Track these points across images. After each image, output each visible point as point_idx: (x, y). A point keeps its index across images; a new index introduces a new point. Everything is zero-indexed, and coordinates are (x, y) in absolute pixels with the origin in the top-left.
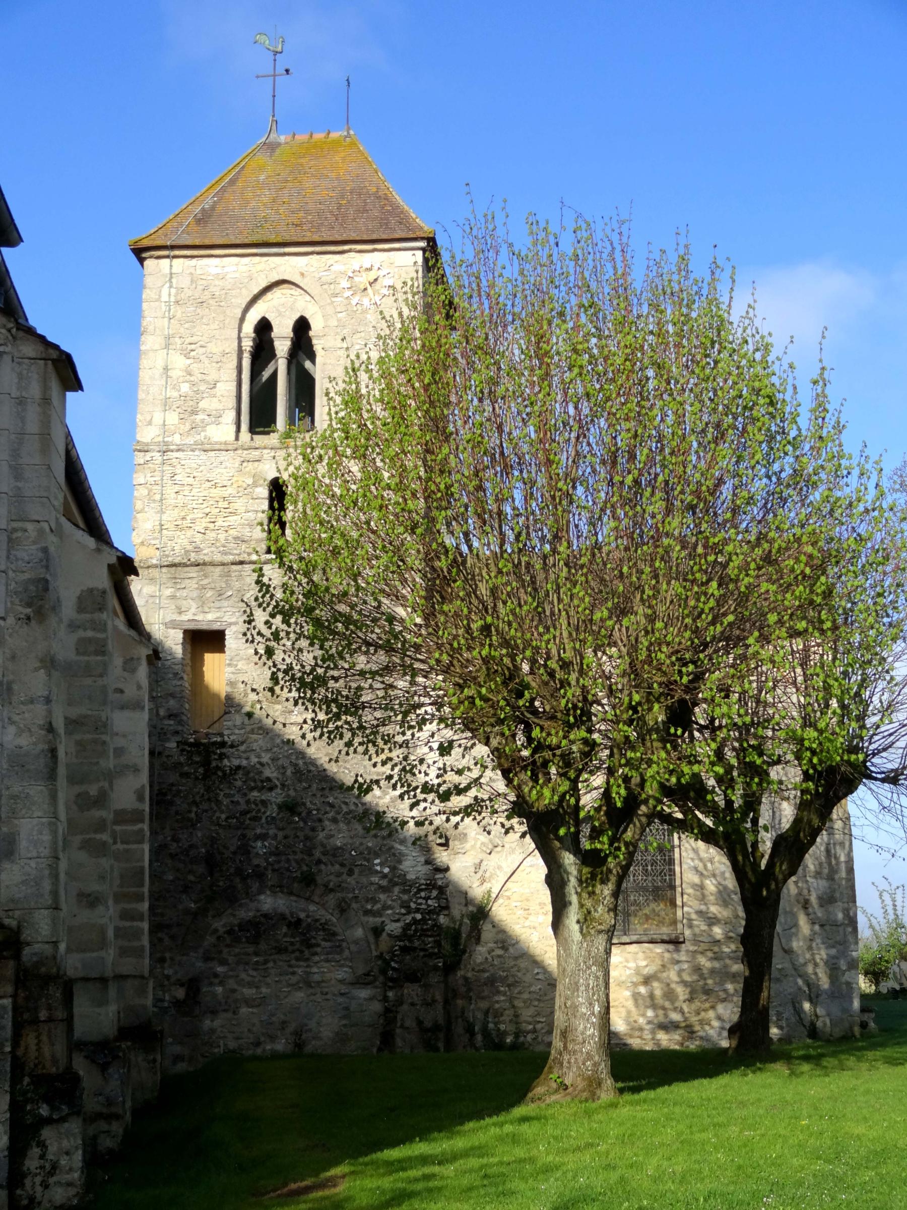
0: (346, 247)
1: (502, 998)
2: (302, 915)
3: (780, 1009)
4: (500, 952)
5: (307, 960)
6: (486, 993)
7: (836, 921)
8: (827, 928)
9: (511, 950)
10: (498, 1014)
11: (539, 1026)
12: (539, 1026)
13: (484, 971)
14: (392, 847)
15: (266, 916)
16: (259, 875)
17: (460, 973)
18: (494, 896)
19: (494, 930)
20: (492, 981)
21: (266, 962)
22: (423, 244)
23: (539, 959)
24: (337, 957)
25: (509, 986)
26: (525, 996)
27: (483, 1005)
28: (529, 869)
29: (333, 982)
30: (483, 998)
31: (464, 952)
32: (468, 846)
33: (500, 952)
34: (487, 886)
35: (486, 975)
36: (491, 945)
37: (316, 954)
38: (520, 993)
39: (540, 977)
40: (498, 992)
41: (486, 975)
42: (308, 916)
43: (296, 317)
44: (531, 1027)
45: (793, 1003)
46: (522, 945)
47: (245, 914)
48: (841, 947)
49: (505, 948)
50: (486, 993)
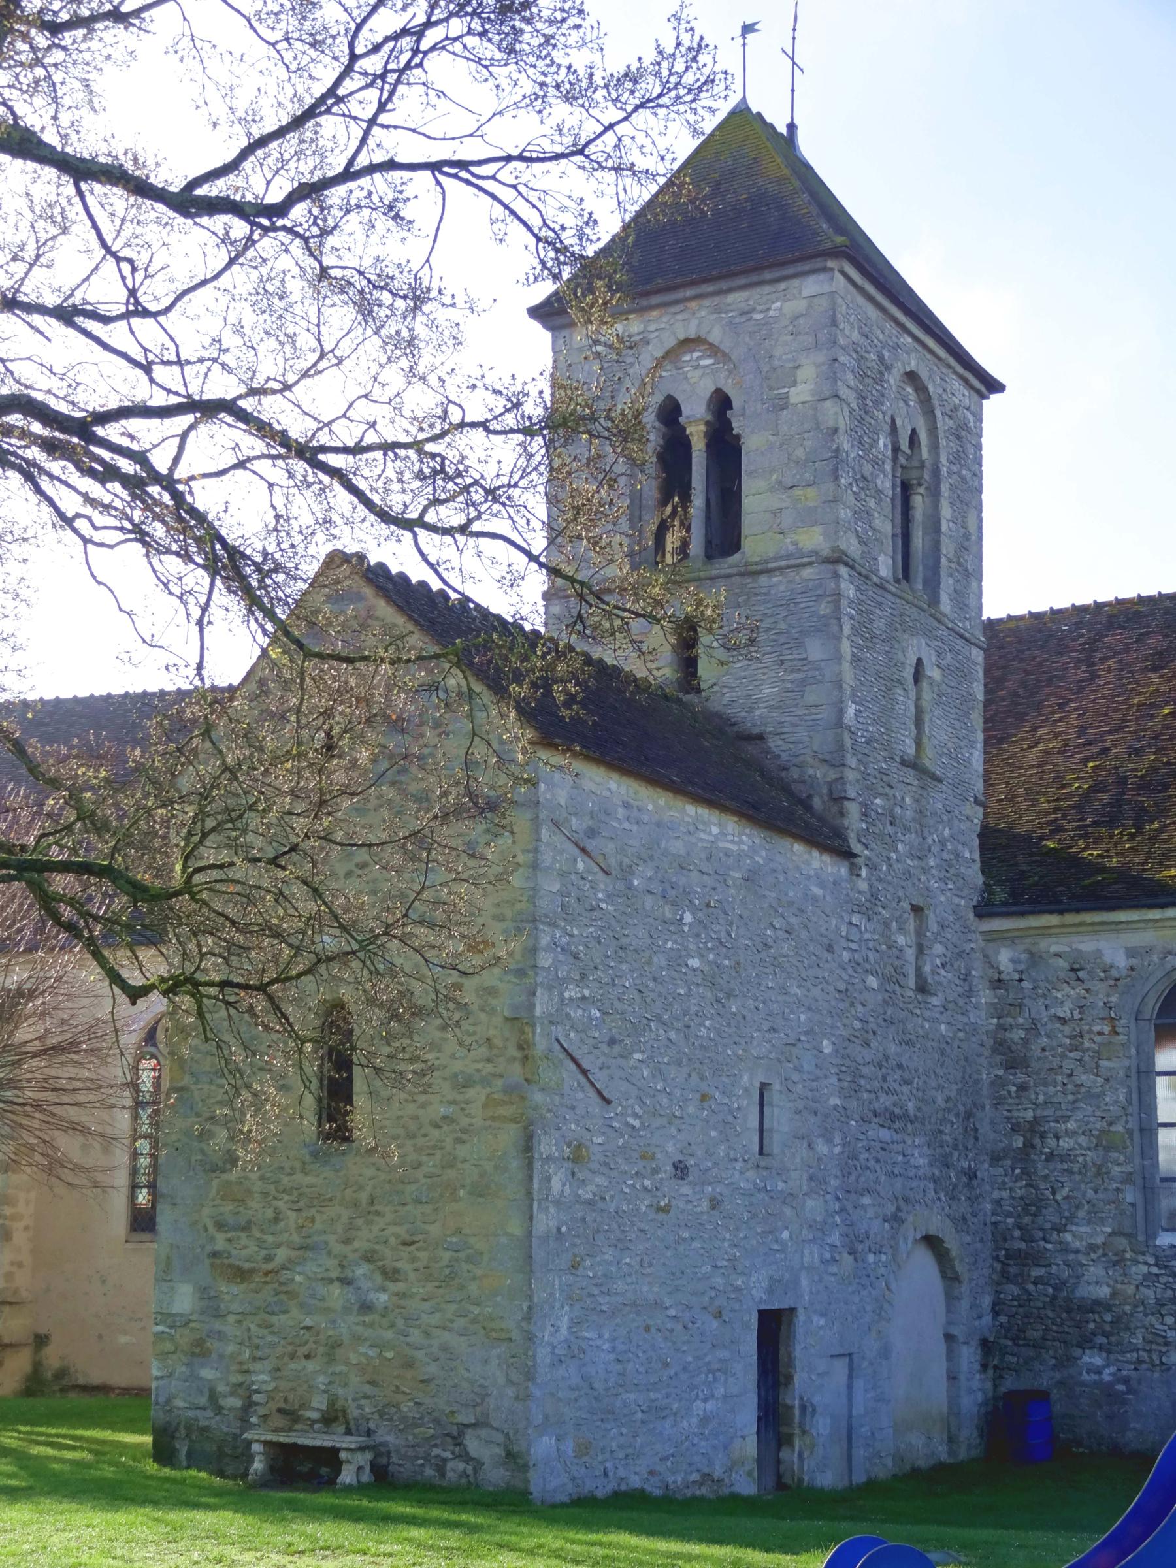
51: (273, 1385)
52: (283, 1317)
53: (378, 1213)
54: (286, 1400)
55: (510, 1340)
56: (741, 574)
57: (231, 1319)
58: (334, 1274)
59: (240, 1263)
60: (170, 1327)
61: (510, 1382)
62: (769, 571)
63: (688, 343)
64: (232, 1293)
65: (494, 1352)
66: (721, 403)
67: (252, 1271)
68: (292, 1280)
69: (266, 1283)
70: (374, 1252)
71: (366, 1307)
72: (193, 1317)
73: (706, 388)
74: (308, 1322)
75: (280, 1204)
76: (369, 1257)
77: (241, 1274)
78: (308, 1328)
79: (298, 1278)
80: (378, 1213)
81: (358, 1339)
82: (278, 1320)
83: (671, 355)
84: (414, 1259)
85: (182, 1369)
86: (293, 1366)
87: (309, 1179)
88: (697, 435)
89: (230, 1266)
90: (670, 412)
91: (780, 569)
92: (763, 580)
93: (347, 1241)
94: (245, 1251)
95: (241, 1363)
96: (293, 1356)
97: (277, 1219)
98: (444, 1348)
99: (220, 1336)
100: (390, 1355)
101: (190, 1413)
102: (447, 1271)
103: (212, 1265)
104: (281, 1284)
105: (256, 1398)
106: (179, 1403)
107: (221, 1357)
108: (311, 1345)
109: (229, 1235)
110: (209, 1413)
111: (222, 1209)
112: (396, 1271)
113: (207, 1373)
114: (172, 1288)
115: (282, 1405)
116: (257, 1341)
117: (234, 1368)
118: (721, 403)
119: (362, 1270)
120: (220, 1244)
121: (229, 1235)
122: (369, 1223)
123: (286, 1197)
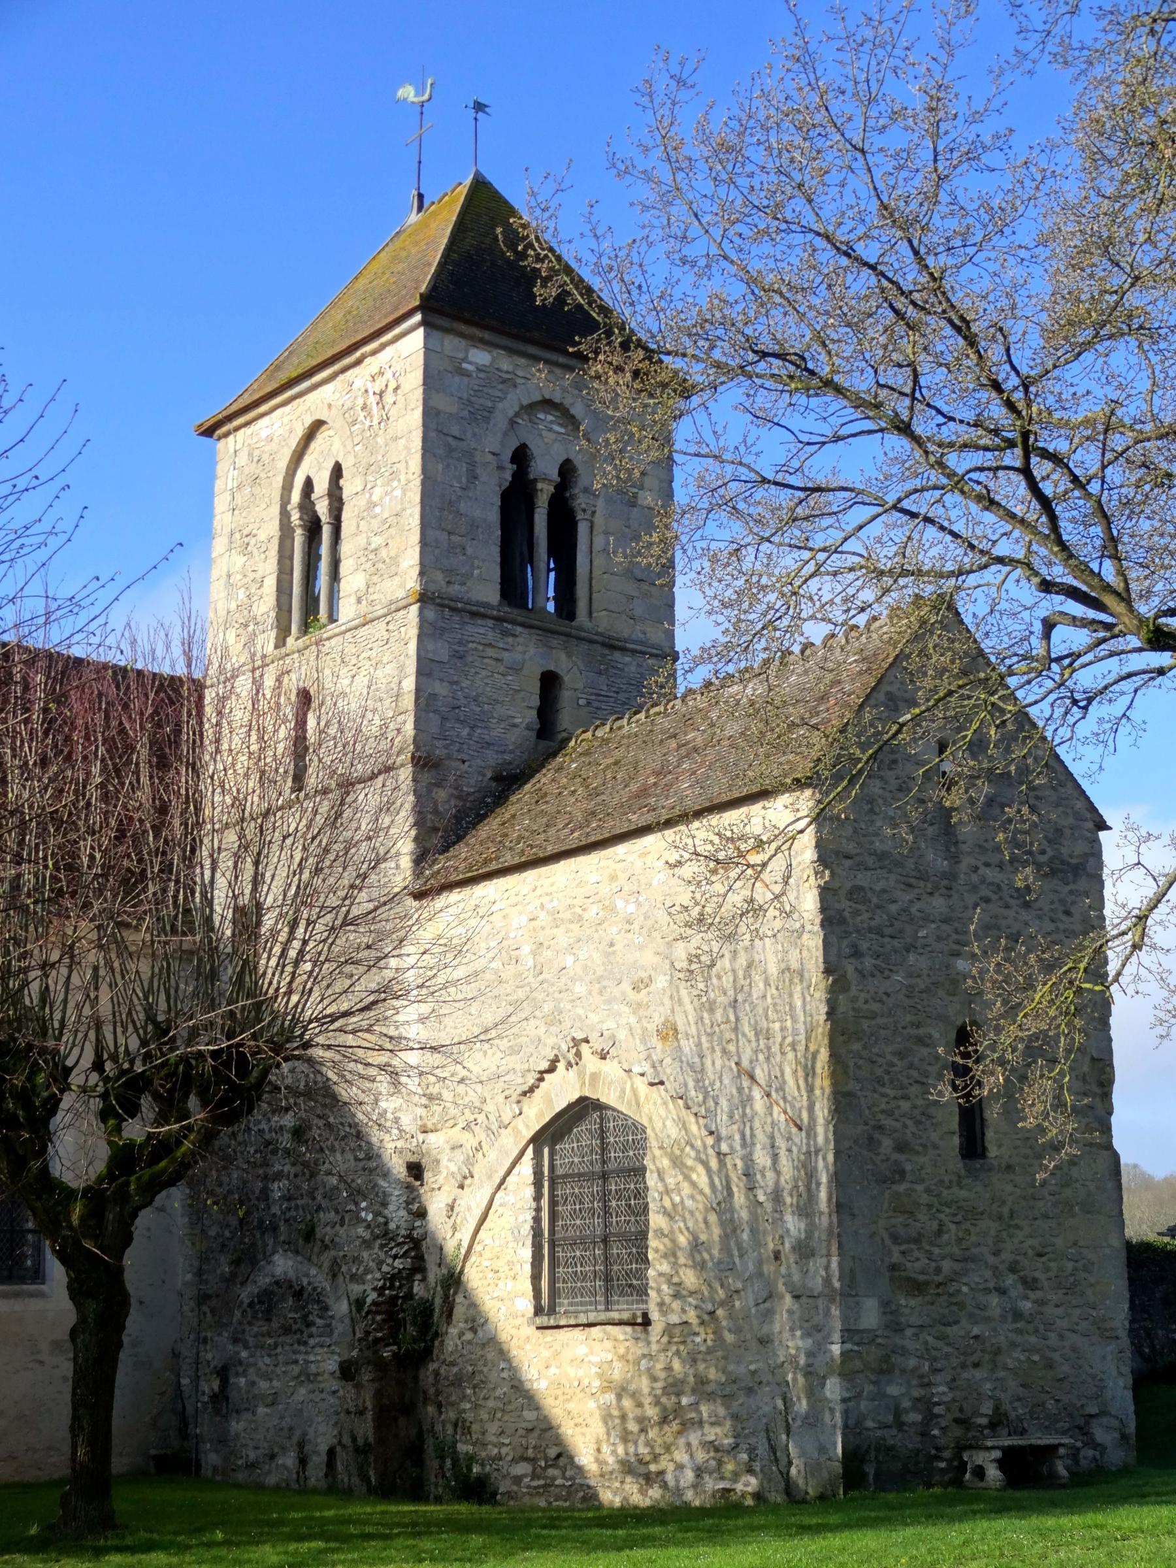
0: (358, 354)
1: (468, 1406)
2: (305, 1281)
3: (752, 1441)
4: (469, 1336)
5: (305, 1343)
6: (453, 1398)
7: (812, 1290)
8: (804, 1300)
9: (480, 1334)
10: (466, 1429)
11: (504, 1450)
12: (504, 1450)
13: (453, 1364)
14: (376, 1185)
15: (277, 1283)
16: (274, 1228)
17: (432, 1366)
18: (463, 1251)
19: (466, 1302)
20: (458, 1382)
21: (276, 1346)
22: (418, 317)
23: (505, 1347)
24: (328, 1341)
25: (474, 1387)
26: (491, 1404)
27: (452, 1415)
28: (501, 1210)
29: (326, 1376)
30: (452, 1404)
31: (436, 1335)
32: (441, 1178)
33: (469, 1336)
34: (458, 1235)
35: (455, 1370)
36: (462, 1325)
37: (311, 1336)
38: (485, 1399)
39: (505, 1375)
40: (464, 1397)
41: (455, 1370)
42: (309, 1283)
43: (332, 464)
44: (496, 1451)
45: (767, 1430)
46: (491, 1326)
47: (264, 1281)
48: (819, 1336)
49: (473, 1330)
50: (453, 1398)
51: (951, 1395)
52: (955, 1328)
53: (1017, 1227)
54: (961, 1410)
55: (1117, 1338)
56: (604, 645)
57: (909, 1332)
58: (991, 1285)
59: (913, 1275)
60: (858, 1344)
61: (1120, 1374)
62: (623, 650)
63: (547, 404)
64: (910, 1307)
65: (1109, 1349)
66: (567, 470)
67: (927, 1284)
68: (959, 1291)
69: (938, 1294)
70: (1016, 1262)
71: (1018, 1315)
72: (879, 1333)
73: (559, 453)
74: (976, 1331)
75: (942, 1216)
76: (1013, 1269)
77: (917, 1287)
78: (976, 1337)
79: (965, 1289)
80: (1017, 1227)
81: (1013, 1345)
82: (952, 1331)
83: (531, 408)
84: (1048, 1270)
85: (869, 1388)
86: (965, 1375)
87: (964, 1194)
88: (545, 492)
89: (908, 1279)
90: (521, 456)
91: (634, 651)
92: (617, 655)
93: (997, 1253)
94: (916, 1266)
95: (921, 1377)
96: (963, 1366)
97: (940, 1232)
98: (1074, 1349)
99: (904, 1352)
100: (1036, 1358)
101: (879, 1433)
102: (1072, 1279)
103: (892, 1279)
104: (951, 1295)
105: (937, 1410)
106: (870, 1424)
107: (903, 1371)
108: (979, 1354)
109: (904, 1247)
110: (894, 1431)
111: (893, 1221)
112: (1035, 1280)
113: (893, 1390)
114: (857, 1303)
115: (957, 1415)
116: (934, 1353)
117: (914, 1382)
118: (567, 470)
119: (1010, 1280)
120: (896, 1257)
121: (904, 1247)
122: (1011, 1236)
123: (947, 1210)
